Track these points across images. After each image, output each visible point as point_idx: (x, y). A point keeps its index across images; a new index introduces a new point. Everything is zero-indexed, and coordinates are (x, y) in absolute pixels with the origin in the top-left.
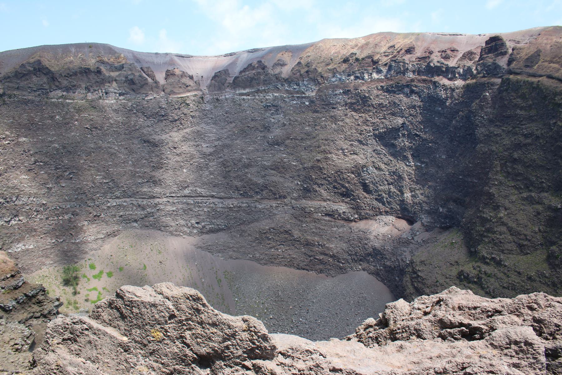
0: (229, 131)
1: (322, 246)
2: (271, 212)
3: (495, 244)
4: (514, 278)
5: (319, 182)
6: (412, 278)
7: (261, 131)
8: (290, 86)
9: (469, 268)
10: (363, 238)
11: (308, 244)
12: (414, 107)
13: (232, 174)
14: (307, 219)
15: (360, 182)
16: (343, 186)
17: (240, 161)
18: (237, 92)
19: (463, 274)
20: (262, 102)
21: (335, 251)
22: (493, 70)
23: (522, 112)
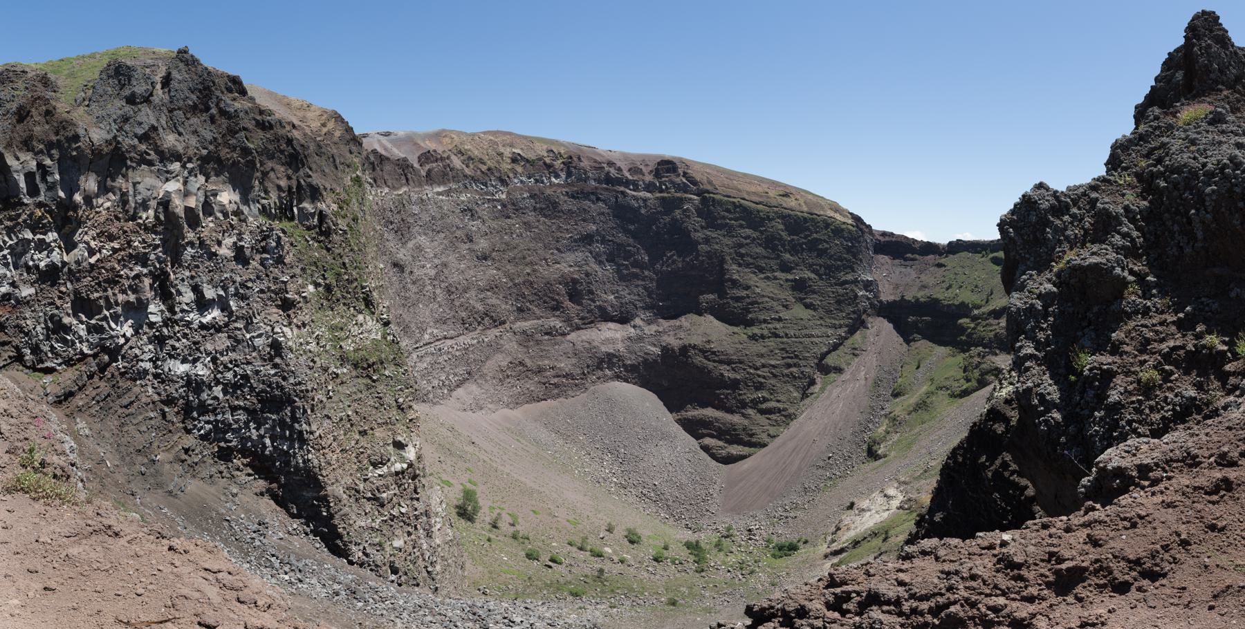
0: (441, 243)
1: (553, 368)
2: (498, 344)
3: (768, 309)
4: (802, 322)
5: (531, 298)
6: (706, 358)
7: (465, 243)
8: (477, 186)
9: (755, 330)
10: (591, 349)
11: (540, 371)
12: (603, 214)
13: (457, 304)
14: (531, 343)
15: (566, 292)
16: (553, 299)
17: (460, 284)
18: (435, 190)
19: (757, 335)
20: (458, 205)
21: (567, 370)
22: (685, 189)
23: (733, 222)
